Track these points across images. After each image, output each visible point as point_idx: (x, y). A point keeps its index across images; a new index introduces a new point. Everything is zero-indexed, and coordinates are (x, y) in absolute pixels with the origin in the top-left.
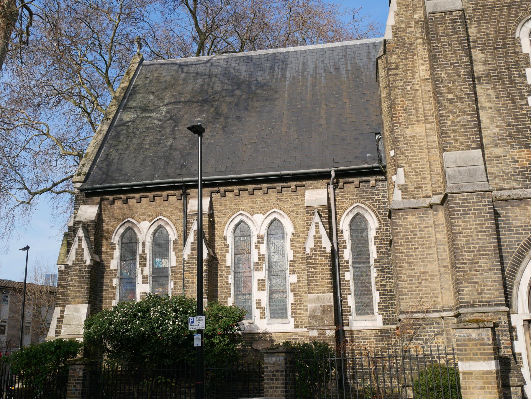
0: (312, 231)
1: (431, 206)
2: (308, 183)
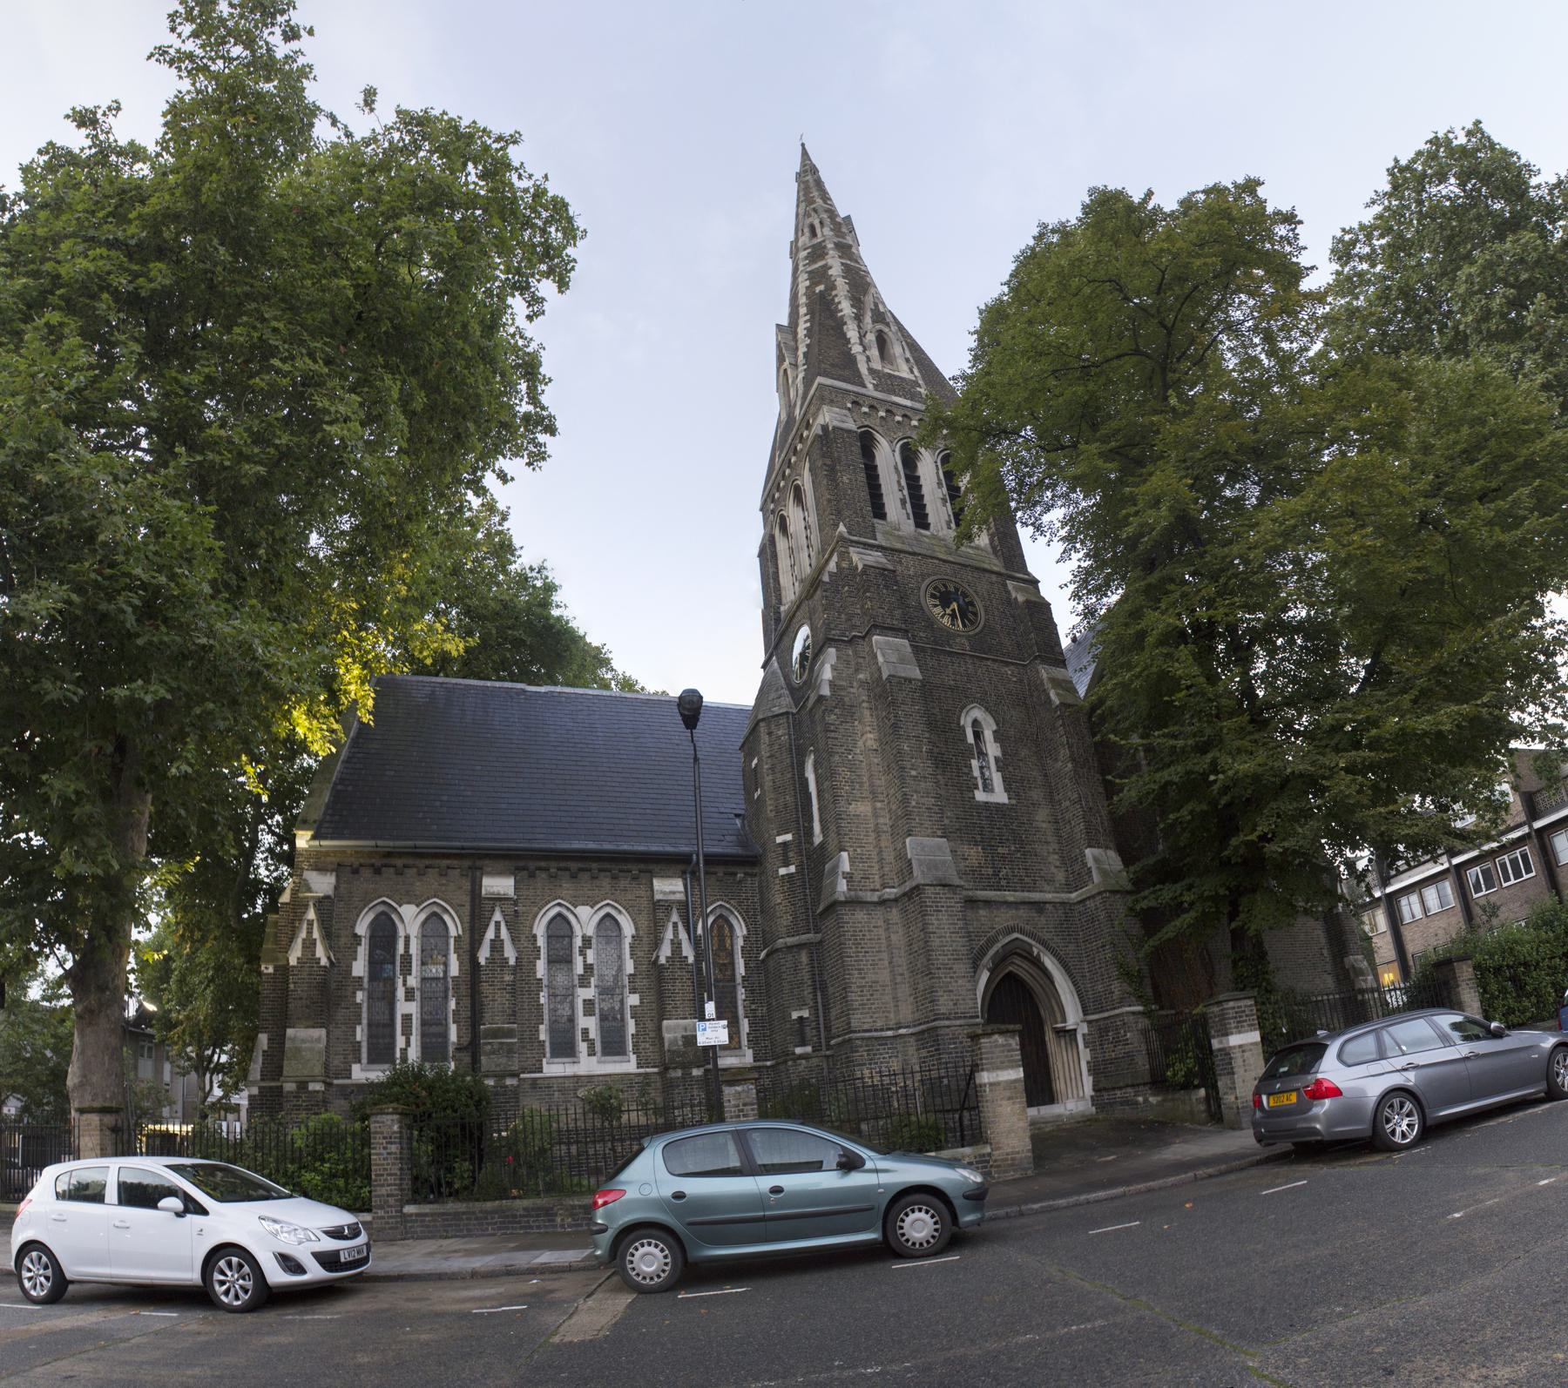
0: (669, 935)
1: (883, 902)
2: (656, 868)
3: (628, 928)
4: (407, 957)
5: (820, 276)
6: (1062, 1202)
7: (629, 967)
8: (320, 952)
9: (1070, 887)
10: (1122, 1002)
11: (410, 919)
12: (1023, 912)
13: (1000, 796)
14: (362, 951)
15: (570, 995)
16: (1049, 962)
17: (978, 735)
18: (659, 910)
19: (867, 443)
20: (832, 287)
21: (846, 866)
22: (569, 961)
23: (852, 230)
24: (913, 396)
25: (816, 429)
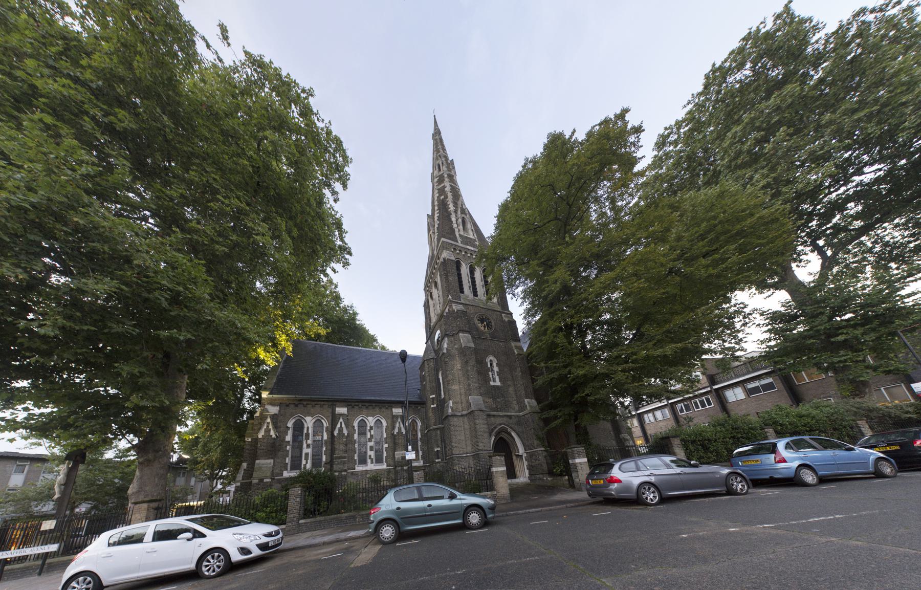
0: (397, 425)
1: (462, 416)
3: (384, 423)
4: (308, 434)
5: (442, 191)
6: (520, 512)
7: (385, 435)
8: (272, 433)
9: (520, 411)
10: (537, 447)
11: (309, 422)
12: (505, 419)
13: (498, 383)
14: (290, 433)
15: (365, 445)
16: (513, 434)
17: (491, 365)
18: (394, 418)
19: (458, 265)
20: (446, 197)
21: (451, 405)
22: (365, 434)
23: (454, 168)
24: (474, 246)
25: (442, 260)
